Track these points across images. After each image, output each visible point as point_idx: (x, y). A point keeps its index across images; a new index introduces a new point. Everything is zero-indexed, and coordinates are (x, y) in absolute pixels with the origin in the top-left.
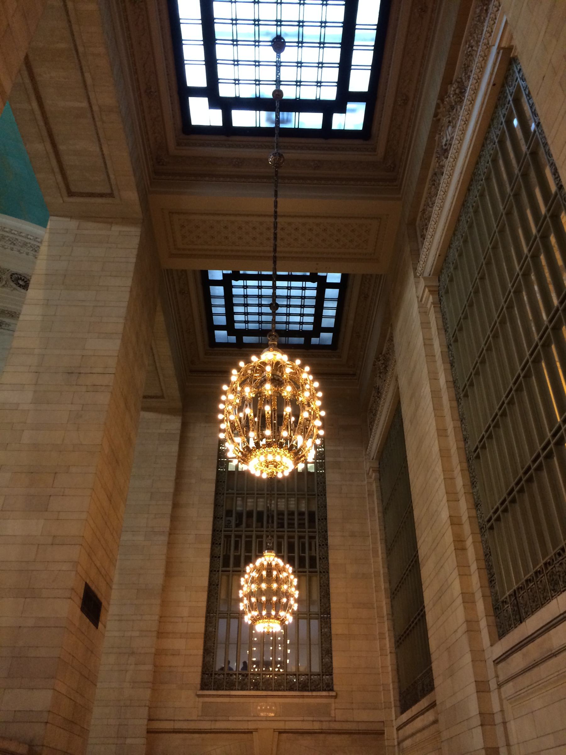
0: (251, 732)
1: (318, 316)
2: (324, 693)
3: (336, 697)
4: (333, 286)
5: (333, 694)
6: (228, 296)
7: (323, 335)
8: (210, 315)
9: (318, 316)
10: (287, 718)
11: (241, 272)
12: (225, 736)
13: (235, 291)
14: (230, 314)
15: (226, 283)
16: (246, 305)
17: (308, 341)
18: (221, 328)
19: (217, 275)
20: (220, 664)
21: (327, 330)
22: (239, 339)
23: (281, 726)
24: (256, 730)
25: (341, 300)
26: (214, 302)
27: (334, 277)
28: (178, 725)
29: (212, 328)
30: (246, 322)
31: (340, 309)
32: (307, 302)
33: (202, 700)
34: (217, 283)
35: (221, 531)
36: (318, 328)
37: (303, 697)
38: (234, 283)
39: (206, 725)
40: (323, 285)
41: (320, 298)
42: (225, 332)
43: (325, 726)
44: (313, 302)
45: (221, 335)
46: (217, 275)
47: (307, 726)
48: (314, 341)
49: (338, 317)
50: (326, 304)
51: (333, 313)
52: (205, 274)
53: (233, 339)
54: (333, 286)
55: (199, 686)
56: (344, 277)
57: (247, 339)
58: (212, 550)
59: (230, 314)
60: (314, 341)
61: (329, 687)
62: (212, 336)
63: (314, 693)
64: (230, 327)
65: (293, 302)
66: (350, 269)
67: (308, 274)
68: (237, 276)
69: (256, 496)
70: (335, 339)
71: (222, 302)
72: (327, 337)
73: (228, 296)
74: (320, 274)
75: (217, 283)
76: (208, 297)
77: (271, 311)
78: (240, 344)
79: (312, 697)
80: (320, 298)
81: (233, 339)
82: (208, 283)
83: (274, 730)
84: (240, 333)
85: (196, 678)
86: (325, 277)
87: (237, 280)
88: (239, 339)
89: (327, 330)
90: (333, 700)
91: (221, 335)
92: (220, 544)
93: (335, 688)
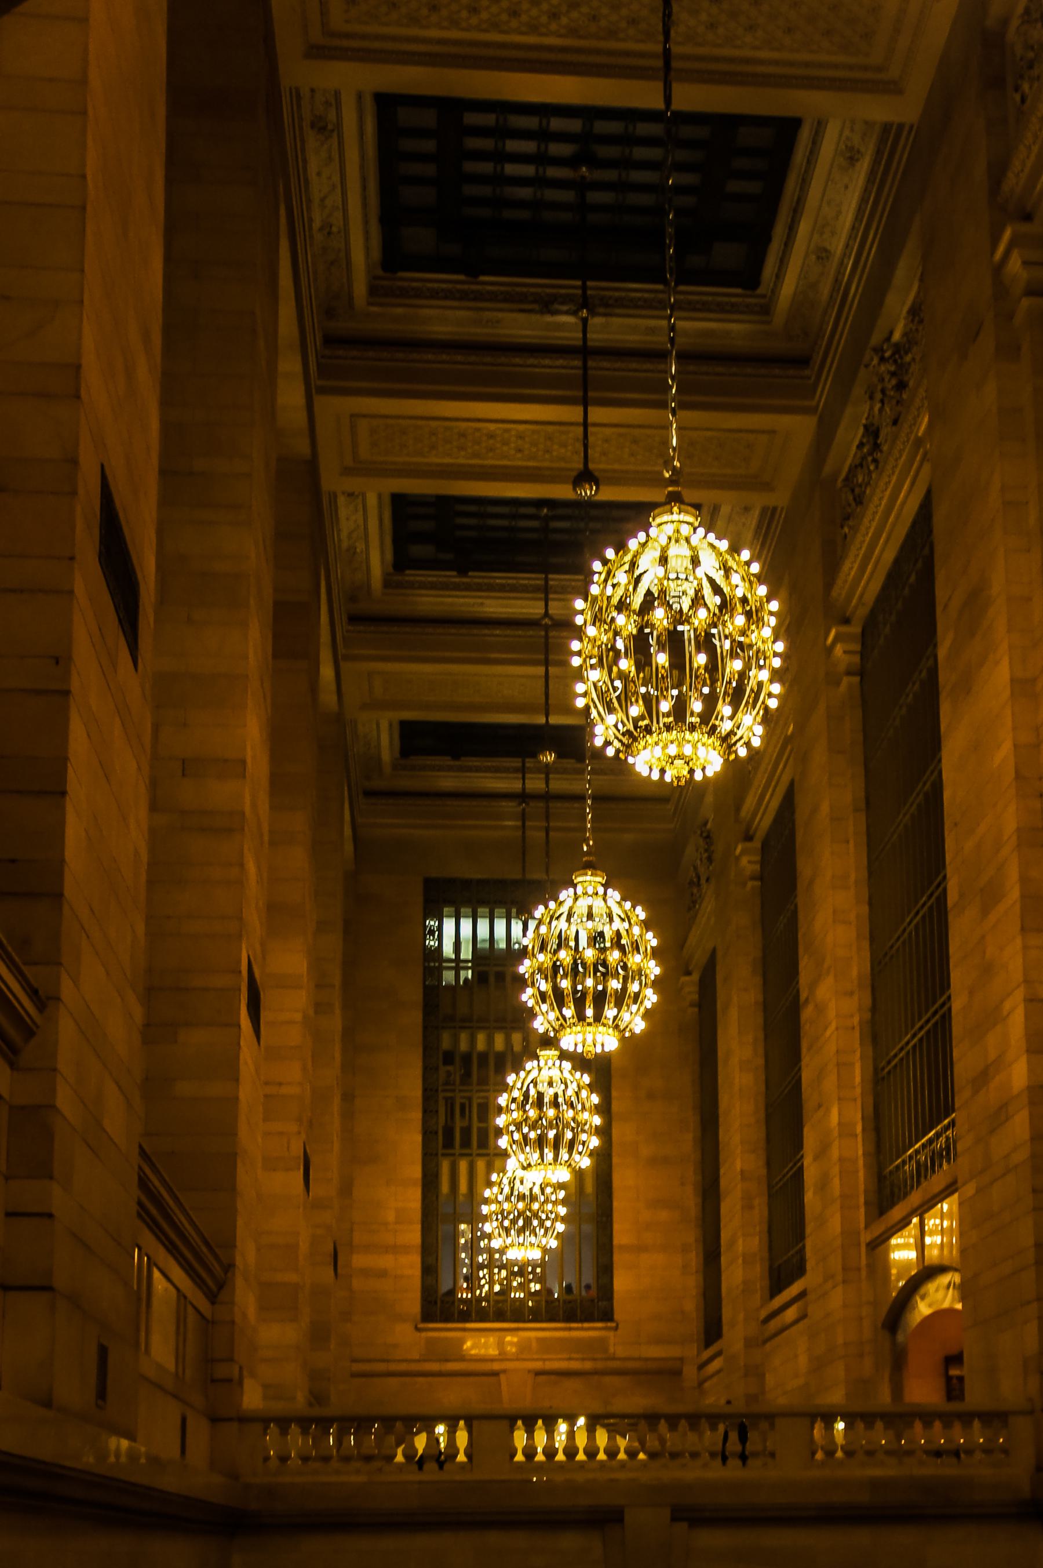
2: (599, 1325)
3: (616, 1328)
5: (613, 1325)
12: (459, 1379)
20: (445, 1286)
23: (538, 1365)
24: (504, 1371)
28: (393, 1367)
33: (424, 1334)
37: (570, 1329)
39: (435, 1367)
43: (600, 1365)
47: (575, 1365)
55: (419, 1317)
61: (607, 1315)
63: (586, 1325)
77: (335, 134)
79: (582, 1329)
83: (529, 1371)
85: (412, 1303)
90: (611, 1334)
93: (616, 1317)
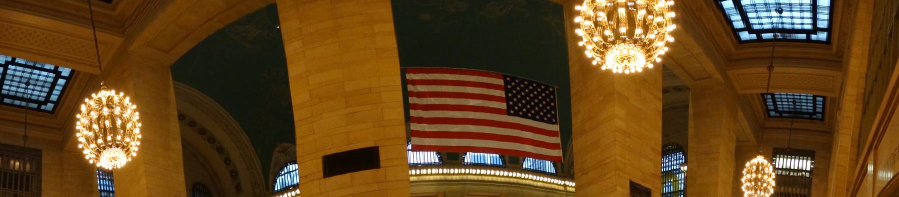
1: (50, 93)
4: (63, 77)
7: (49, 104)
9: (50, 93)
13: (9, 72)
17: (39, 106)
25: (65, 87)
27: (66, 72)
31: (62, 92)
32: (46, 85)
36: (47, 100)
38: (10, 66)
40: (58, 75)
41: (54, 84)
44: (49, 85)
48: (43, 107)
49: (60, 97)
50: (57, 87)
51: (58, 93)
54: (63, 77)
60: (43, 107)
65: (39, 83)
66: (77, 68)
70: (54, 108)
72: (50, 106)
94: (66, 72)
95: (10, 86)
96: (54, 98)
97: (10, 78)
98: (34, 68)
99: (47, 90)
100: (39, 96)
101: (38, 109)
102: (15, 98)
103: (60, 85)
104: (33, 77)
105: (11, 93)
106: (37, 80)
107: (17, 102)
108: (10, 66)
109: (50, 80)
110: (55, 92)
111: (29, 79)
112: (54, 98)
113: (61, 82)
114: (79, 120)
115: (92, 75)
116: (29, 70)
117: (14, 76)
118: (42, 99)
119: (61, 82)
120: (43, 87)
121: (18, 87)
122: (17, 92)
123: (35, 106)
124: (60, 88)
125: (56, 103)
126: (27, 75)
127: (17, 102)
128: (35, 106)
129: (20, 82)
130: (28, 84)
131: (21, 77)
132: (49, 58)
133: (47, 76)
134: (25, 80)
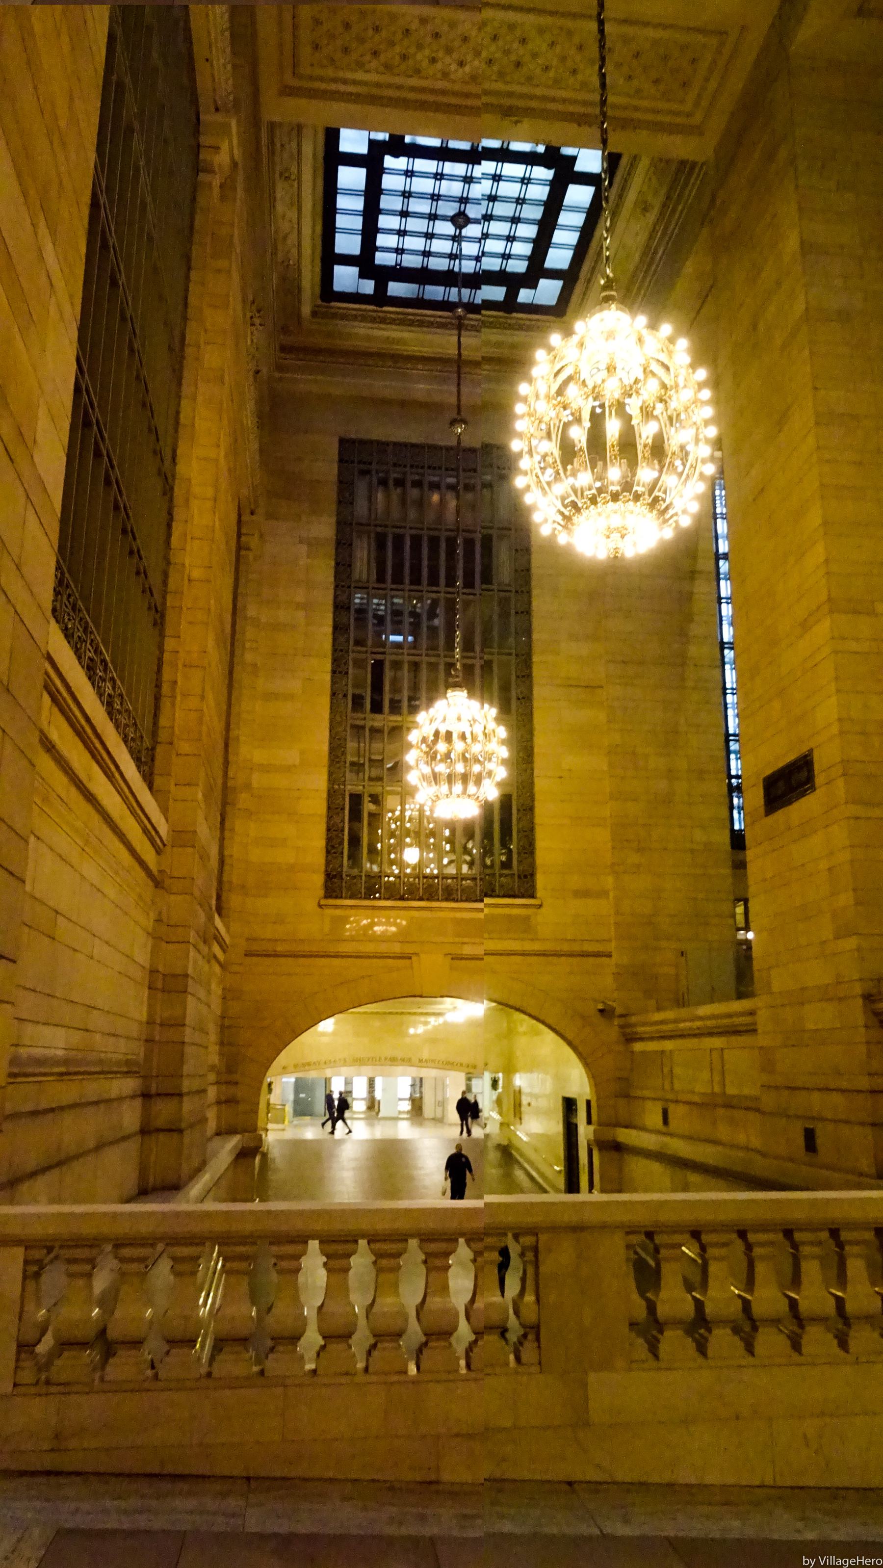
0: (410, 958)
1: (542, 243)
6: (373, 192)
8: (329, 230)
9: (542, 243)
10: (466, 940)
11: (408, 139)
14: (370, 231)
15: (372, 162)
16: (404, 214)
18: (347, 260)
19: (353, 141)
21: (554, 274)
22: (381, 287)
25: (594, 212)
26: (342, 202)
29: (330, 258)
30: (399, 251)
31: (587, 232)
34: (353, 160)
35: (347, 652)
36: (536, 270)
41: (554, 205)
42: (355, 270)
44: (537, 213)
45: (346, 277)
46: (353, 141)
49: (581, 250)
50: (564, 218)
52: (333, 136)
53: (368, 287)
55: (322, 893)
56: (612, 161)
57: (396, 288)
58: (333, 683)
59: (370, 231)
62: (327, 277)
64: (364, 261)
67: (541, 149)
68: (397, 146)
69: (407, 594)
70: (565, 297)
71: (359, 204)
73: (373, 192)
74: (567, 151)
75: (353, 160)
76: (331, 190)
78: (380, 297)
80: (554, 205)
81: (368, 287)
82: (334, 158)
84: (384, 276)
86: (574, 159)
87: (396, 155)
88: (381, 287)
89: (554, 274)
91: (346, 277)
92: (347, 673)
94: (589, 160)
95: (402, 233)
96: (558, 258)
97: (396, 203)
98: (473, 157)
99: (531, 231)
100: (506, 256)
101: (510, 304)
102: (423, 276)
103: (574, 209)
104: (478, 190)
105: (411, 261)
106: (492, 198)
107: (435, 292)
108: (389, 161)
109: (539, 192)
110: (558, 236)
111: (464, 200)
112: (558, 258)
113: (579, 195)
114: (653, 326)
115: (683, 163)
116: (460, 169)
117: (407, 195)
118: (519, 267)
119: (579, 195)
120: (515, 220)
121: (429, 236)
122: (426, 254)
123: (497, 293)
124: (579, 219)
125: (569, 277)
126: (455, 188)
127: (435, 292)
128: (497, 293)
129: (433, 217)
130: (460, 220)
131: (435, 197)
132: (511, 113)
133: (525, 181)
134: (448, 209)
